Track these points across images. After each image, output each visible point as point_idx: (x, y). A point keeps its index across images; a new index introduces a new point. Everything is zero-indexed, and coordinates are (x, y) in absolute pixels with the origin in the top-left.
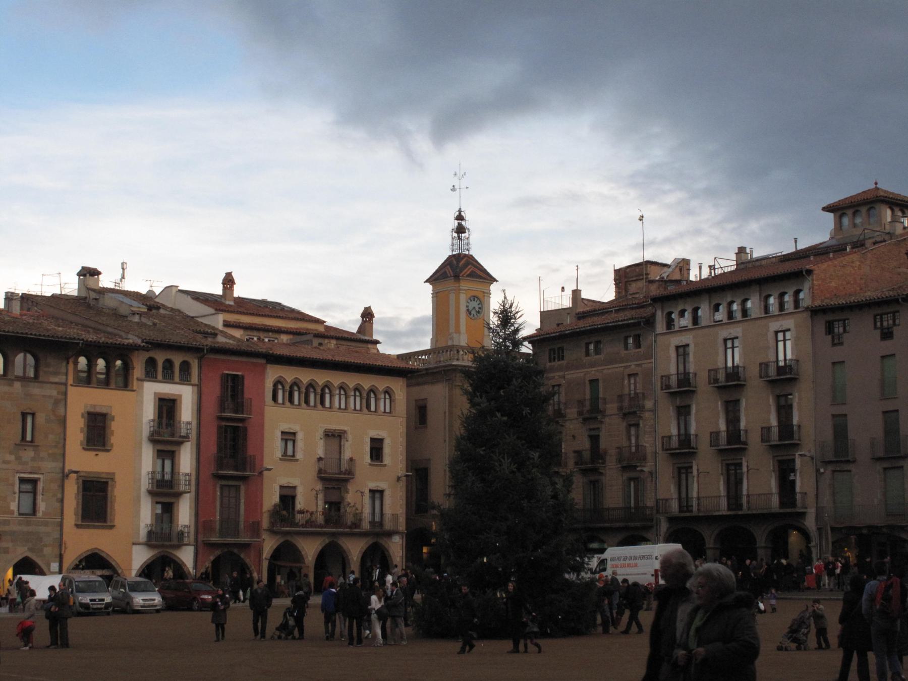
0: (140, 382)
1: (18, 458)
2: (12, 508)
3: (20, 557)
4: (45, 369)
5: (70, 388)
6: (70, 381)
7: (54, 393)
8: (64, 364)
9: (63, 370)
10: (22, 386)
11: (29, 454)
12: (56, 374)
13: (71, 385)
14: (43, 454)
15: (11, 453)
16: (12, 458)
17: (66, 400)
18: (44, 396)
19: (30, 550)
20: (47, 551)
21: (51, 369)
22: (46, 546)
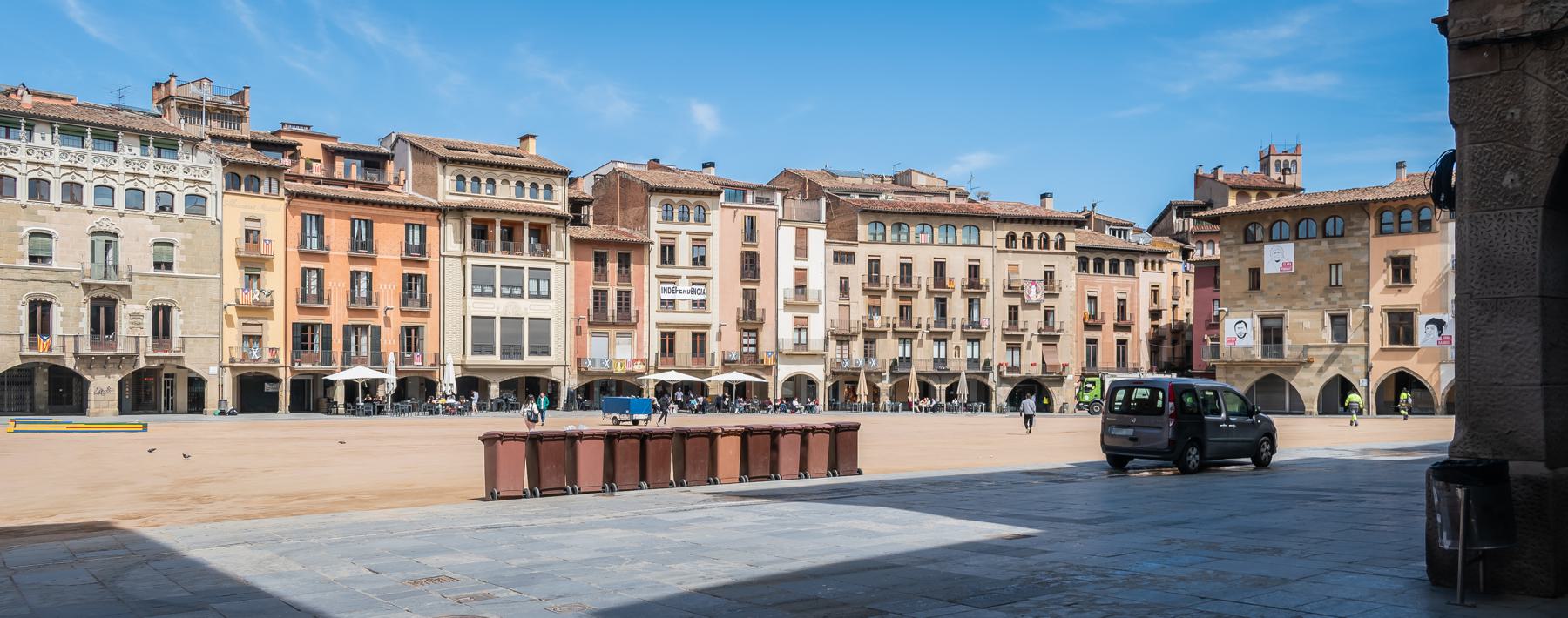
0: (1444, 225)
1: (1328, 300)
2: (1324, 338)
3: (1333, 375)
4: (1349, 227)
5: (1371, 239)
6: (1372, 232)
7: (1359, 245)
8: (1367, 219)
9: (1366, 225)
10: (1329, 243)
11: (1336, 296)
12: (1361, 229)
13: (1373, 237)
14: (1349, 295)
15: (1321, 296)
16: (1323, 299)
17: (1369, 249)
18: (1350, 249)
19: (1340, 369)
20: (1356, 370)
21: (1354, 227)
22: (1355, 366)
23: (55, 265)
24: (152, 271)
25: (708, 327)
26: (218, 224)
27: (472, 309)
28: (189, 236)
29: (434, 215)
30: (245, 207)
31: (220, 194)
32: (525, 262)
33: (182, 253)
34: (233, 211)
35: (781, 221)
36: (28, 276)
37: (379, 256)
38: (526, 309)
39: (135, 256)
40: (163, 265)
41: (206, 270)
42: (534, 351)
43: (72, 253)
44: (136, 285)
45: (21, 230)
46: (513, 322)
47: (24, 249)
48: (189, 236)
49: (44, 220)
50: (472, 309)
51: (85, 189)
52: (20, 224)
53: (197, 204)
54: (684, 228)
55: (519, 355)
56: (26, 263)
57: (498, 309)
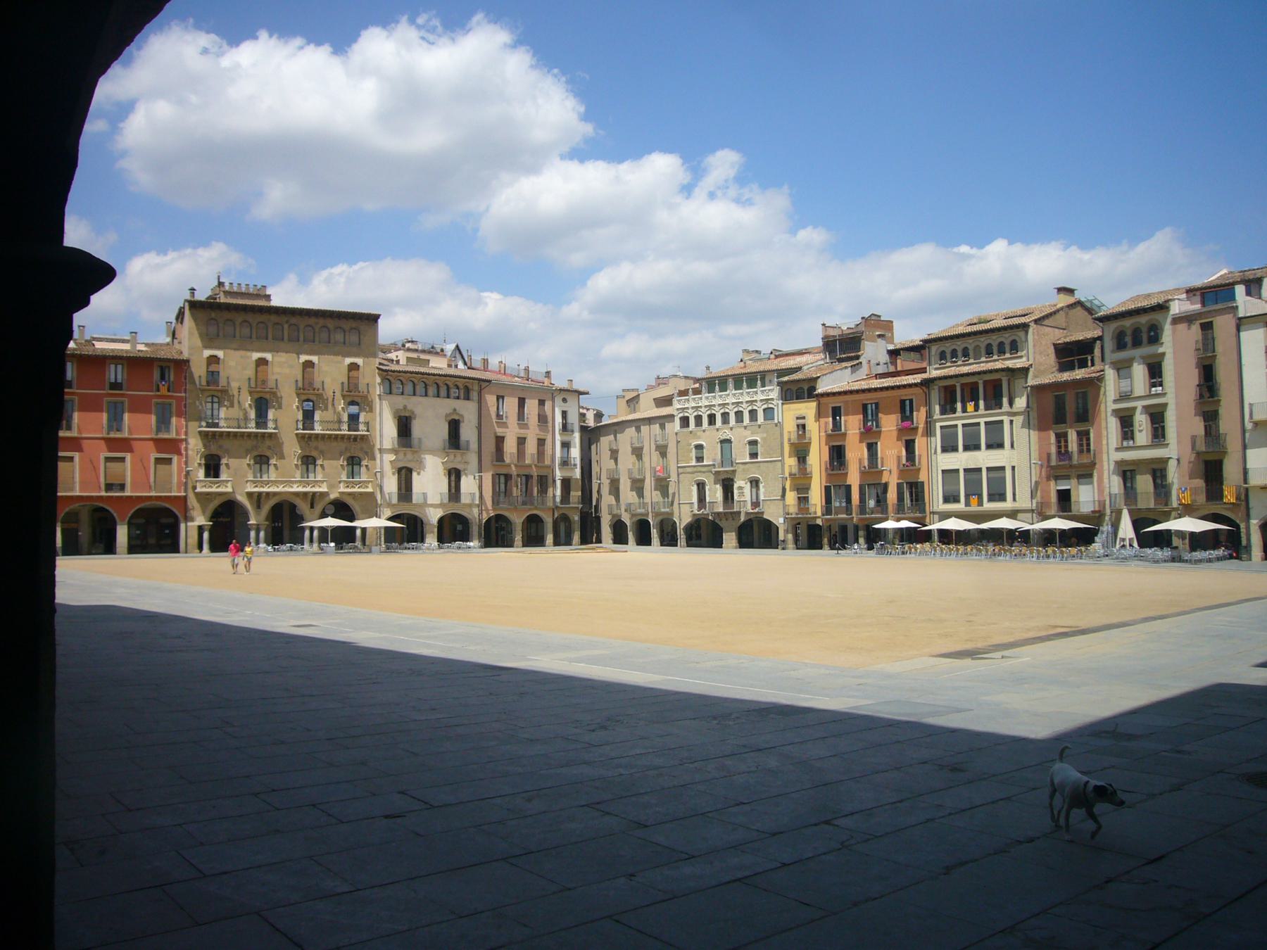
23: (705, 463)
24: (748, 460)
25: (1165, 461)
26: (779, 425)
27: (941, 464)
28: (765, 435)
29: (918, 390)
30: (796, 410)
31: (780, 405)
32: (981, 416)
33: (762, 446)
34: (789, 414)
35: (1240, 319)
36: (695, 469)
37: (883, 429)
38: (984, 460)
39: (741, 454)
40: (754, 455)
41: (775, 456)
42: (992, 498)
43: (712, 455)
44: (740, 469)
45: (691, 445)
46: (973, 472)
47: (693, 454)
48: (765, 435)
49: (699, 438)
50: (941, 464)
51: (744, 414)
52: (690, 441)
53: (769, 412)
54: (1138, 352)
55: (980, 503)
56: (694, 463)
57: (961, 461)
